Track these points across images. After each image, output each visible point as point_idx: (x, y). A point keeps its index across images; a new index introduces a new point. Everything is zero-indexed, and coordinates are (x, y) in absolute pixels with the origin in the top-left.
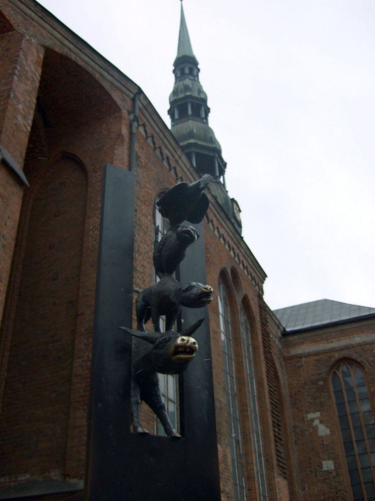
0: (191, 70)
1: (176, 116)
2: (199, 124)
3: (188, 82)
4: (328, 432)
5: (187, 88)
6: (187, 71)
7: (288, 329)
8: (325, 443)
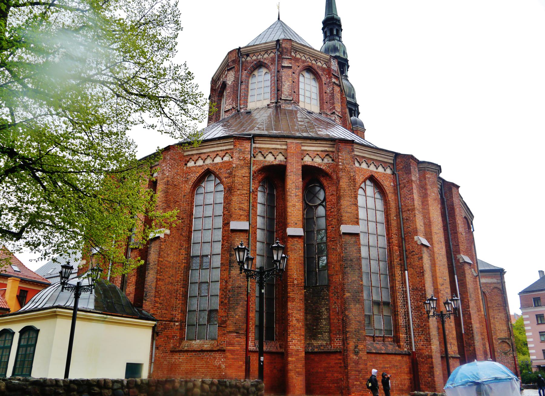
5: (335, 49)
6: (335, 33)
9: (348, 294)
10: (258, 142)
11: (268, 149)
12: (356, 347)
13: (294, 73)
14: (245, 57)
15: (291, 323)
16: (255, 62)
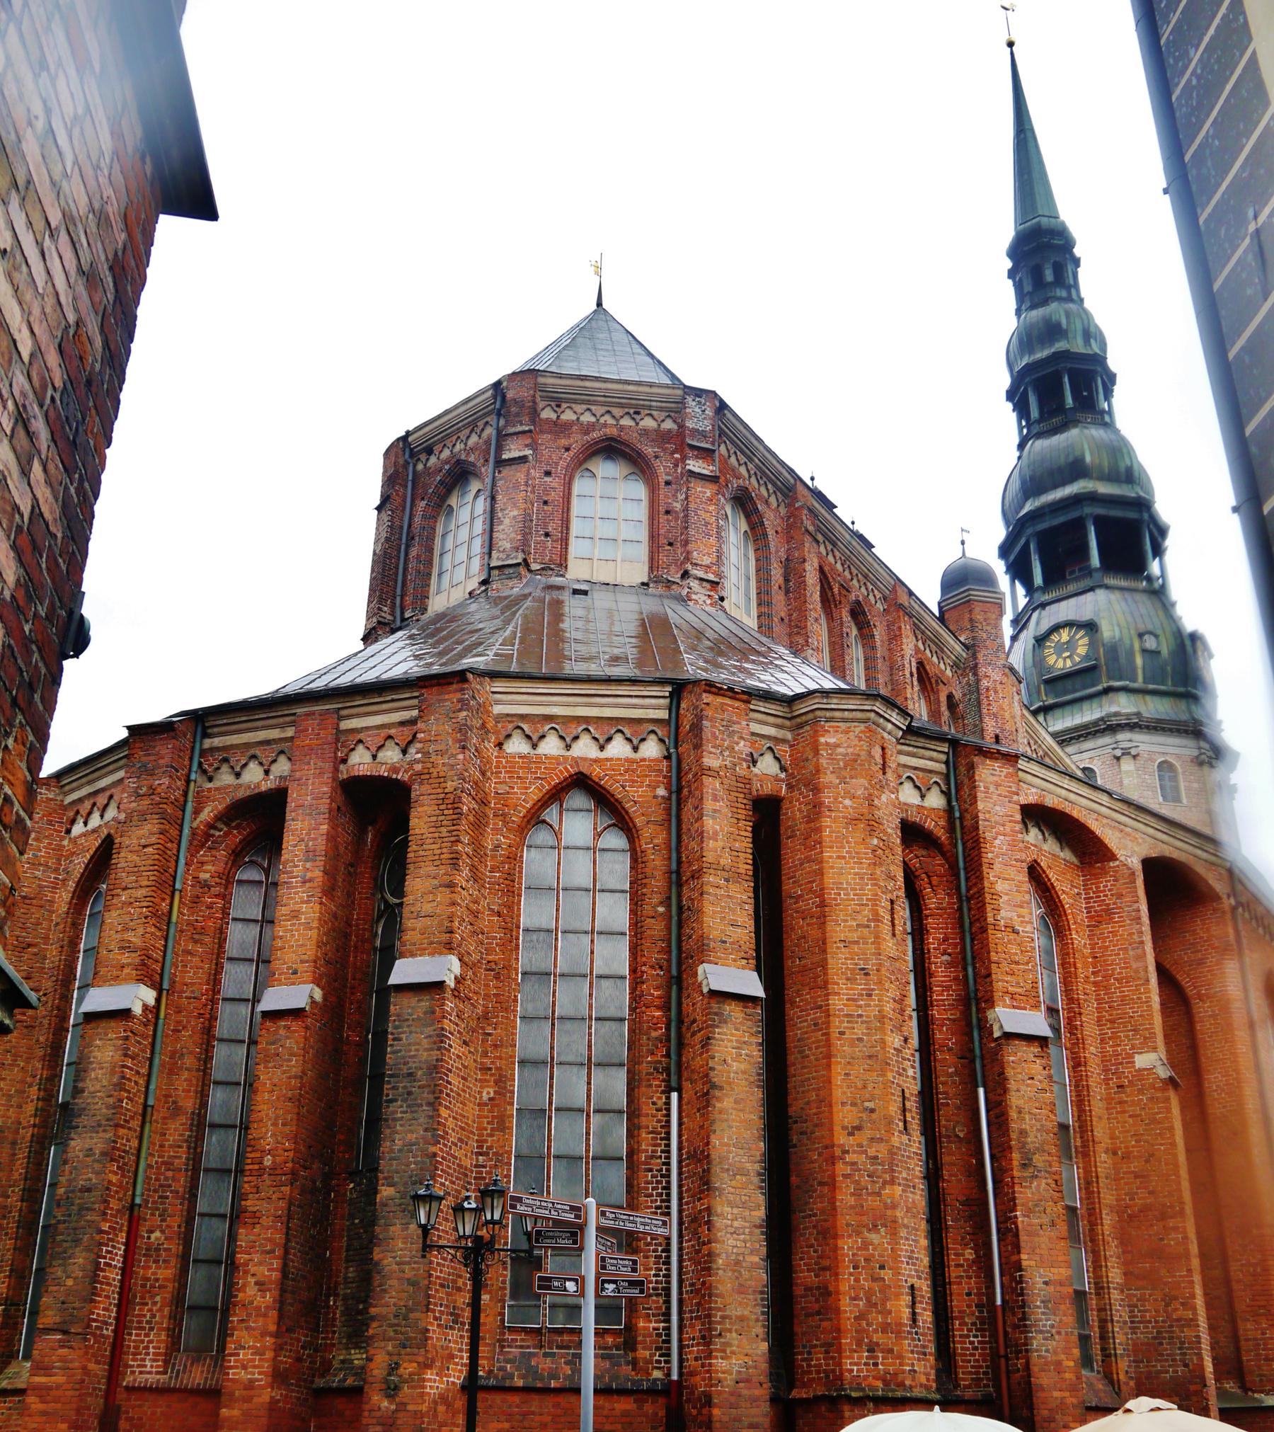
2: (1097, 433)
5: (1052, 331)
9: (386, 1192)
10: (216, 730)
11: (247, 745)
12: (393, 1368)
13: (548, 473)
14: (423, 457)
15: (241, 1295)
16: (447, 467)
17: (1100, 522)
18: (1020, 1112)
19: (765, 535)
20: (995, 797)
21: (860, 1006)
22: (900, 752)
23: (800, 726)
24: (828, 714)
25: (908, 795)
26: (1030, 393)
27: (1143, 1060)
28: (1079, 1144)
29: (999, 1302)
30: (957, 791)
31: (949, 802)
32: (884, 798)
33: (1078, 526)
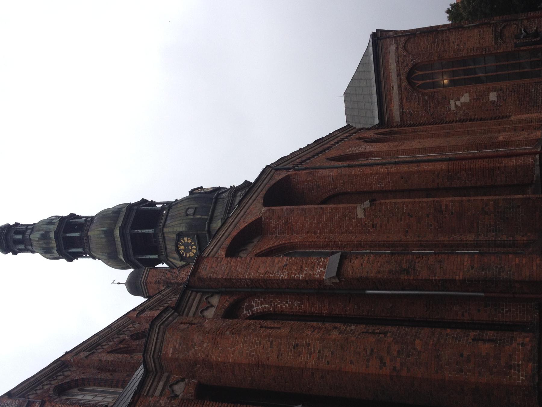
0: (18, 232)
1: (80, 250)
3: (35, 236)
4: (467, 95)
5: (45, 237)
6: (20, 237)
7: (377, 121)
8: (475, 97)
17: (133, 228)
18: (379, 272)
19: (83, 379)
20: (217, 269)
21: (314, 351)
22: (187, 315)
23: (161, 367)
24: (157, 351)
25: (210, 313)
26: (71, 251)
27: (361, 214)
28: (401, 249)
29: (482, 294)
30: (212, 288)
31: (217, 293)
32: (207, 326)
33: (134, 237)
